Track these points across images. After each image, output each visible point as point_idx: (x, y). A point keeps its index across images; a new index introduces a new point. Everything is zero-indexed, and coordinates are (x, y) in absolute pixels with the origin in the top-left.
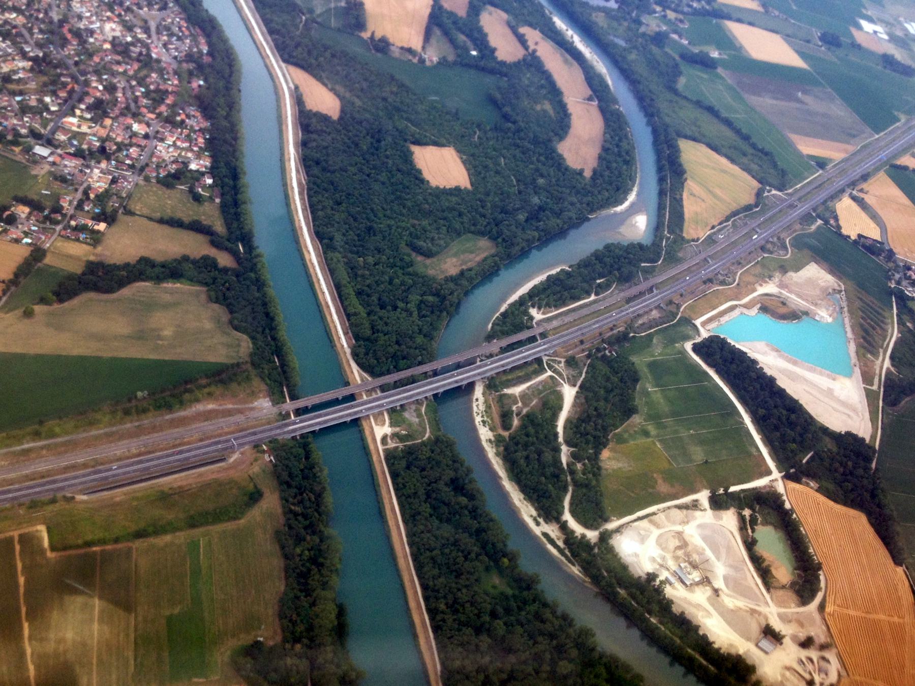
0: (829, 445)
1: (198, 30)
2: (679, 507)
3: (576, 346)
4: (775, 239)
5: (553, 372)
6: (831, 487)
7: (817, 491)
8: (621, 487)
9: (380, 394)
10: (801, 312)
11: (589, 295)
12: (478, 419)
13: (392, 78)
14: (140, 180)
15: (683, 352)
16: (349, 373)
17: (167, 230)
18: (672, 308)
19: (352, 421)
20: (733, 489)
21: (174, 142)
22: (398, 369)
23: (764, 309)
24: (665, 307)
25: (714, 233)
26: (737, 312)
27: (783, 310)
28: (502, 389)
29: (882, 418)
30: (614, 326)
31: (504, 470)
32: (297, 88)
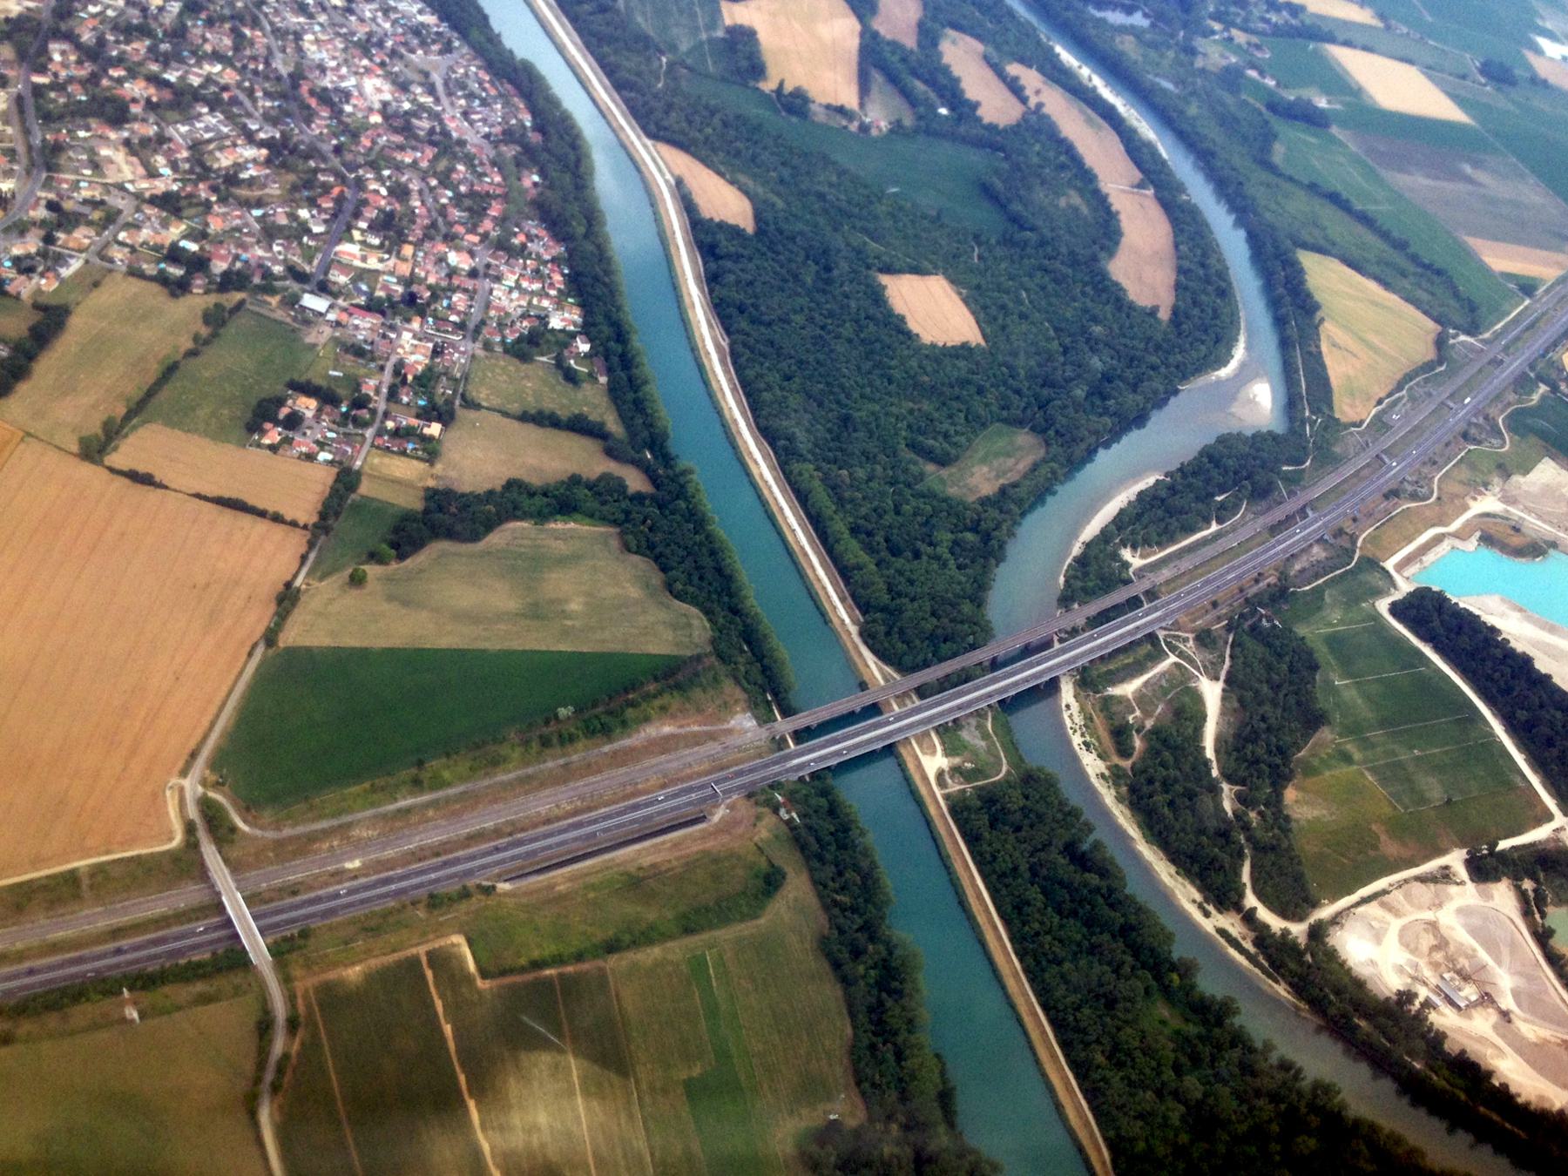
1: (509, 87)
2: (1421, 879)
4: (1481, 420)
11: (1209, 526)
12: (1077, 740)
14: (477, 348)
15: (1377, 617)
17: (533, 432)
18: (1344, 542)
20: (1503, 845)
21: (517, 281)
23: (1487, 540)
24: (1332, 541)
25: (1384, 412)
26: (1445, 546)
27: (1516, 541)
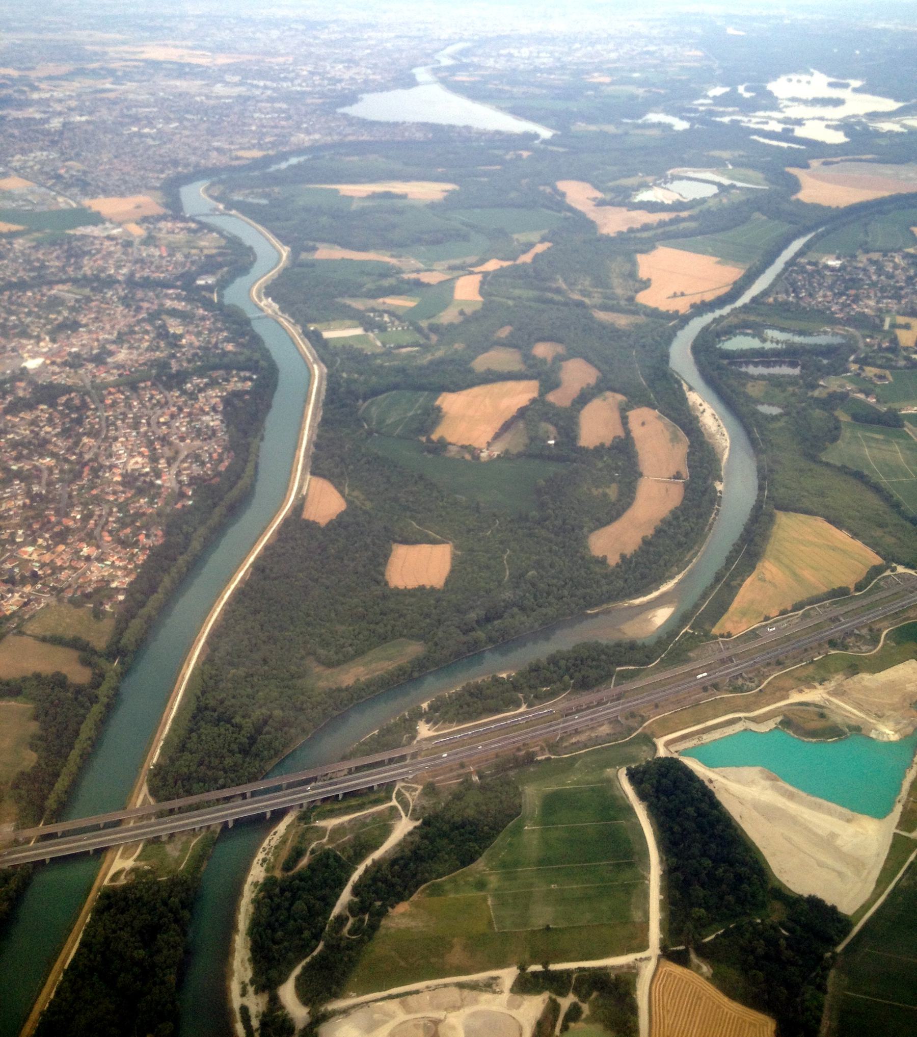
0: (777, 913)
2: (461, 986)
3: (452, 770)
4: (864, 631)
5: (399, 802)
6: (733, 974)
7: (707, 979)
8: (393, 953)
9: (153, 820)
10: (849, 727)
11: (519, 706)
12: (260, 856)
13: (421, 477)
14: (53, 601)
16: (135, 794)
17: (46, 648)
18: (632, 722)
19: (95, 850)
20: (554, 967)
21: (113, 562)
22: (189, 793)
23: (786, 724)
24: (623, 721)
25: (766, 626)
26: (738, 727)
27: (818, 724)
28: (315, 820)
29: (901, 879)
30: (524, 745)
31: (248, 922)
32: (304, 499)
